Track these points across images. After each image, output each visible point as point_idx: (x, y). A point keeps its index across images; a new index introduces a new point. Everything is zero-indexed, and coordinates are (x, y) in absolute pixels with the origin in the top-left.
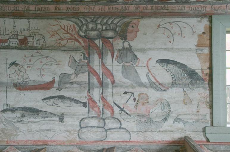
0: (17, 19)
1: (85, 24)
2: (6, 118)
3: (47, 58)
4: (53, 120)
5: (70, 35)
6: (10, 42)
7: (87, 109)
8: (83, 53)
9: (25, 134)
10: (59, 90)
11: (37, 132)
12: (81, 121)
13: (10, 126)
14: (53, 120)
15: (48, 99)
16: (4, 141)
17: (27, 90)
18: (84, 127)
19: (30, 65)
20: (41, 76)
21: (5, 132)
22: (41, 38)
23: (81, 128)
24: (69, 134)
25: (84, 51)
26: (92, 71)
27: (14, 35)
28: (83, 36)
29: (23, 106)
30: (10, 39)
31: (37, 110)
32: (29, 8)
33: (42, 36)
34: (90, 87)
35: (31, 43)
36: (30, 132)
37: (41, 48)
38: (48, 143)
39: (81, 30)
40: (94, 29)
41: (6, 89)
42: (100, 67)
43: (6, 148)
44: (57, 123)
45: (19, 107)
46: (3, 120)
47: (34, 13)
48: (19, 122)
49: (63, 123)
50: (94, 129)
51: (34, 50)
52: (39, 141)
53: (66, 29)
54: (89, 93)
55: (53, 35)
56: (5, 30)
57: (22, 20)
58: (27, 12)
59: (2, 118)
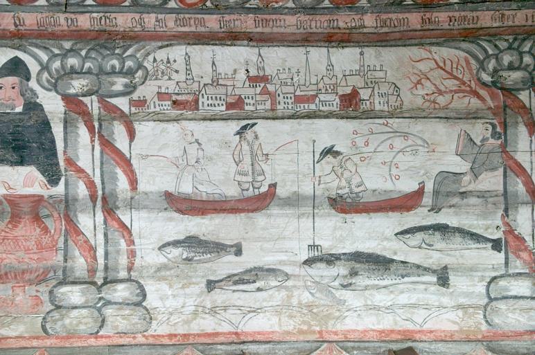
0: (334, 49)
1: (492, 55)
2: (315, 278)
3: (406, 138)
4: (424, 283)
5: (457, 82)
6: (319, 101)
7: (502, 255)
8: (491, 124)
10: (436, 212)
11: (387, 311)
12: (490, 283)
13: (325, 298)
14: (424, 283)
15: (409, 233)
17: (360, 213)
18: (496, 299)
19: (365, 155)
20: (391, 179)
21: (314, 311)
22: (391, 91)
23: (491, 300)
24: (463, 315)
25: (492, 119)
26: (514, 164)
27: (328, 86)
28: (490, 84)
29: (353, 251)
30: (319, 95)
31: (385, 258)
32: (362, 21)
33: (393, 86)
34: (508, 203)
35: (368, 103)
37: (391, 115)
38: (415, 335)
39: (484, 70)
40: (516, 66)
42: (531, 155)
44: (433, 288)
45: (343, 252)
46: (309, 283)
48: (344, 286)
49: (447, 288)
50: (522, 302)
51: (375, 118)
52: (392, 331)
53: (448, 68)
54: (506, 218)
55: (419, 82)
56: (308, 74)
57: (347, 50)
58: (358, 31)
59: (306, 278)
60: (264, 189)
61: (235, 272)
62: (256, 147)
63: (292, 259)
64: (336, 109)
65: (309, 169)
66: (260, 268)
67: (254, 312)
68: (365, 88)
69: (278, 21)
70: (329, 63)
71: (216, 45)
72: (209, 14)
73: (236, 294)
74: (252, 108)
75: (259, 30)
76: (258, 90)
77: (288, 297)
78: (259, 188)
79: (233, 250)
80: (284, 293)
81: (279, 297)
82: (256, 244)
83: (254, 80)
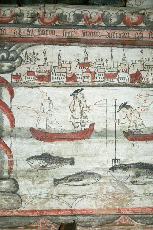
0: (127, 49)
2: (116, 178)
6: (119, 77)
9: (141, 199)
16: (116, 209)
19: (145, 108)
21: (116, 197)
27: (123, 69)
30: (119, 74)
32: (142, 34)
35: (146, 79)
36: (148, 197)
41: (115, 140)
43: (118, 218)
46: (113, 181)
47: (147, 41)
48: (133, 183)
51: (150, 87)
56: (112, 62)
57: (133, 50)
58: (140, 39)
59: (111, 178)
60: (87, 127)
61: (70, 174)
62: (83, 103)
63: (103, 167)
64: (128, 82)
65: (113, 115)
66: (85, 172)
67: (81, 197)
68: (144, 70)
69: (96, 33)
70: (124, 57)
71: (61, 45)
72: (58, 28)
73: (71, 187)
74: (81, 80)
75: (86, 37)
76: (84, 70)
77: (101, 189)
78: (84, 126)
79: (69, 161)
80: (98, 187)
81: (95, 189)
82: (82, 158)
83: (82, 65)
